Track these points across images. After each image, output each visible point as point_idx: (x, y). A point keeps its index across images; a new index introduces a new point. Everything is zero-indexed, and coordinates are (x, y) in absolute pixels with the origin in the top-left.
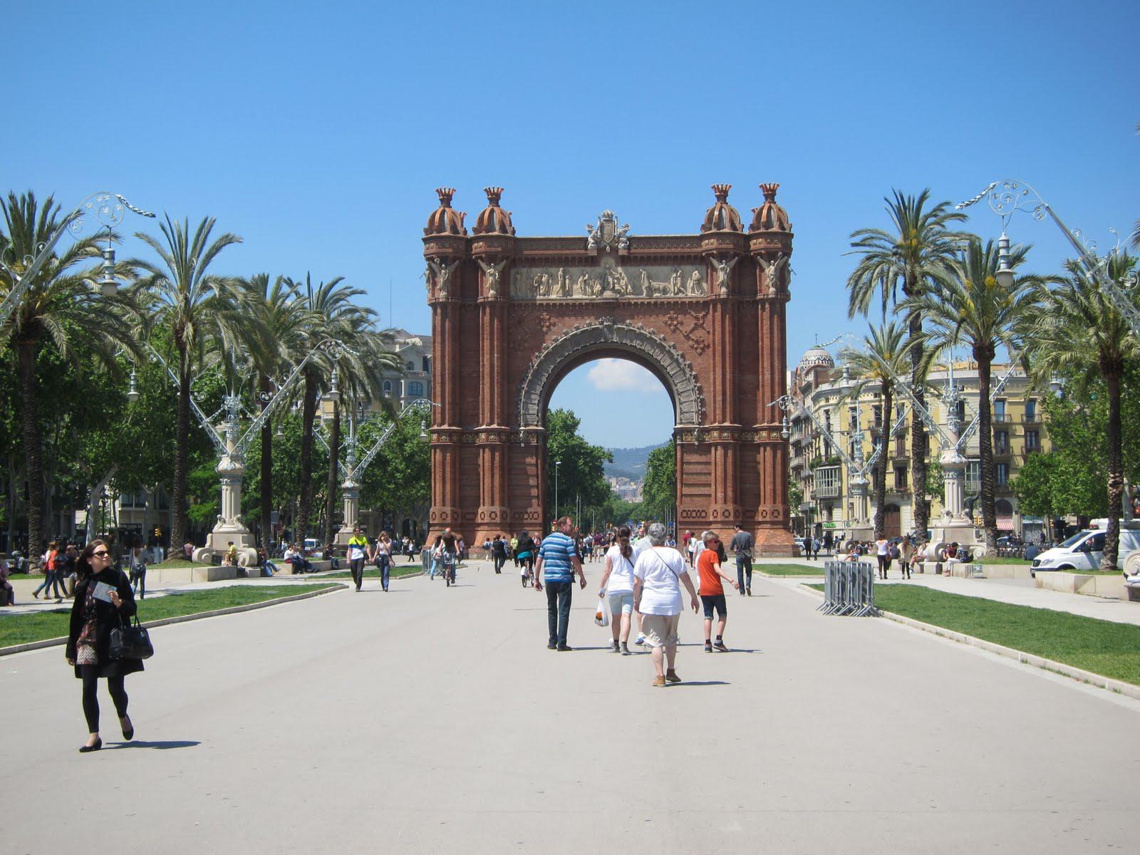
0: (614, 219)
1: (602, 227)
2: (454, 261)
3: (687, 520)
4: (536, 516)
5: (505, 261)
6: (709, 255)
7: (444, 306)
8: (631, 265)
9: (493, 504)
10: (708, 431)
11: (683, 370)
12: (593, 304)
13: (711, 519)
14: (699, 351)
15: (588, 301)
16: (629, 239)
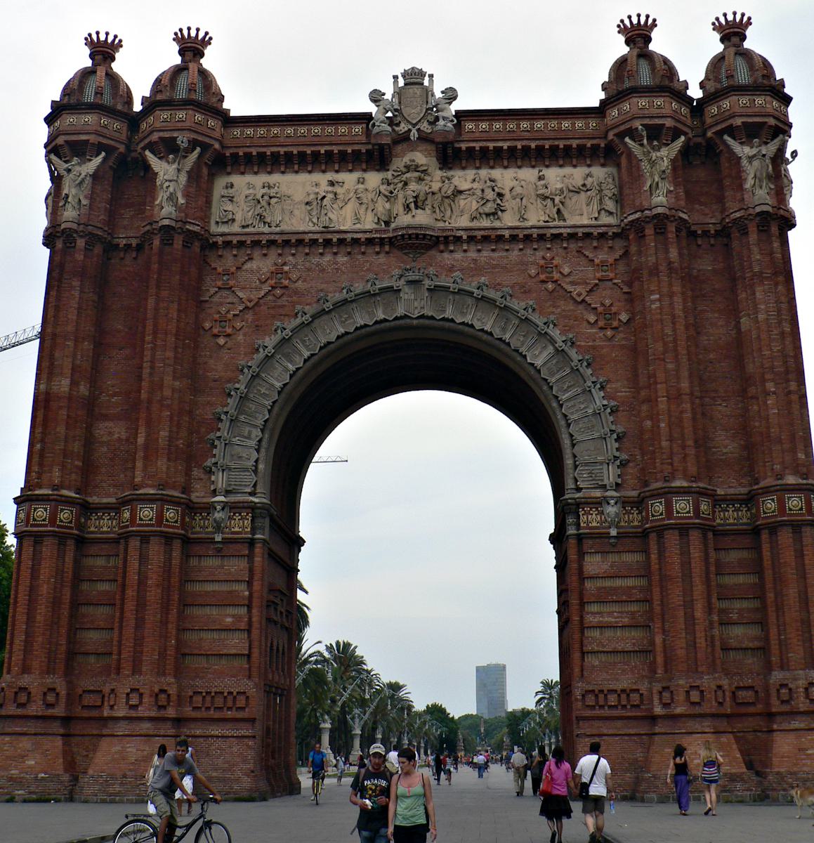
0: (426, 82)
1: (399, 93)
2: (97, 155)
3: (598, 712)
4: (241, 702)
5: (198, 149)
6: (621, 136)
7: (68, 236)
8: (464, 168)
9: (136, 670)
10: (639, 503)
11: (575, 371)
12: (380, 238)
13: (658, 710)
14: (609, 333)
15: (368, 235)
16: (460, 115)
